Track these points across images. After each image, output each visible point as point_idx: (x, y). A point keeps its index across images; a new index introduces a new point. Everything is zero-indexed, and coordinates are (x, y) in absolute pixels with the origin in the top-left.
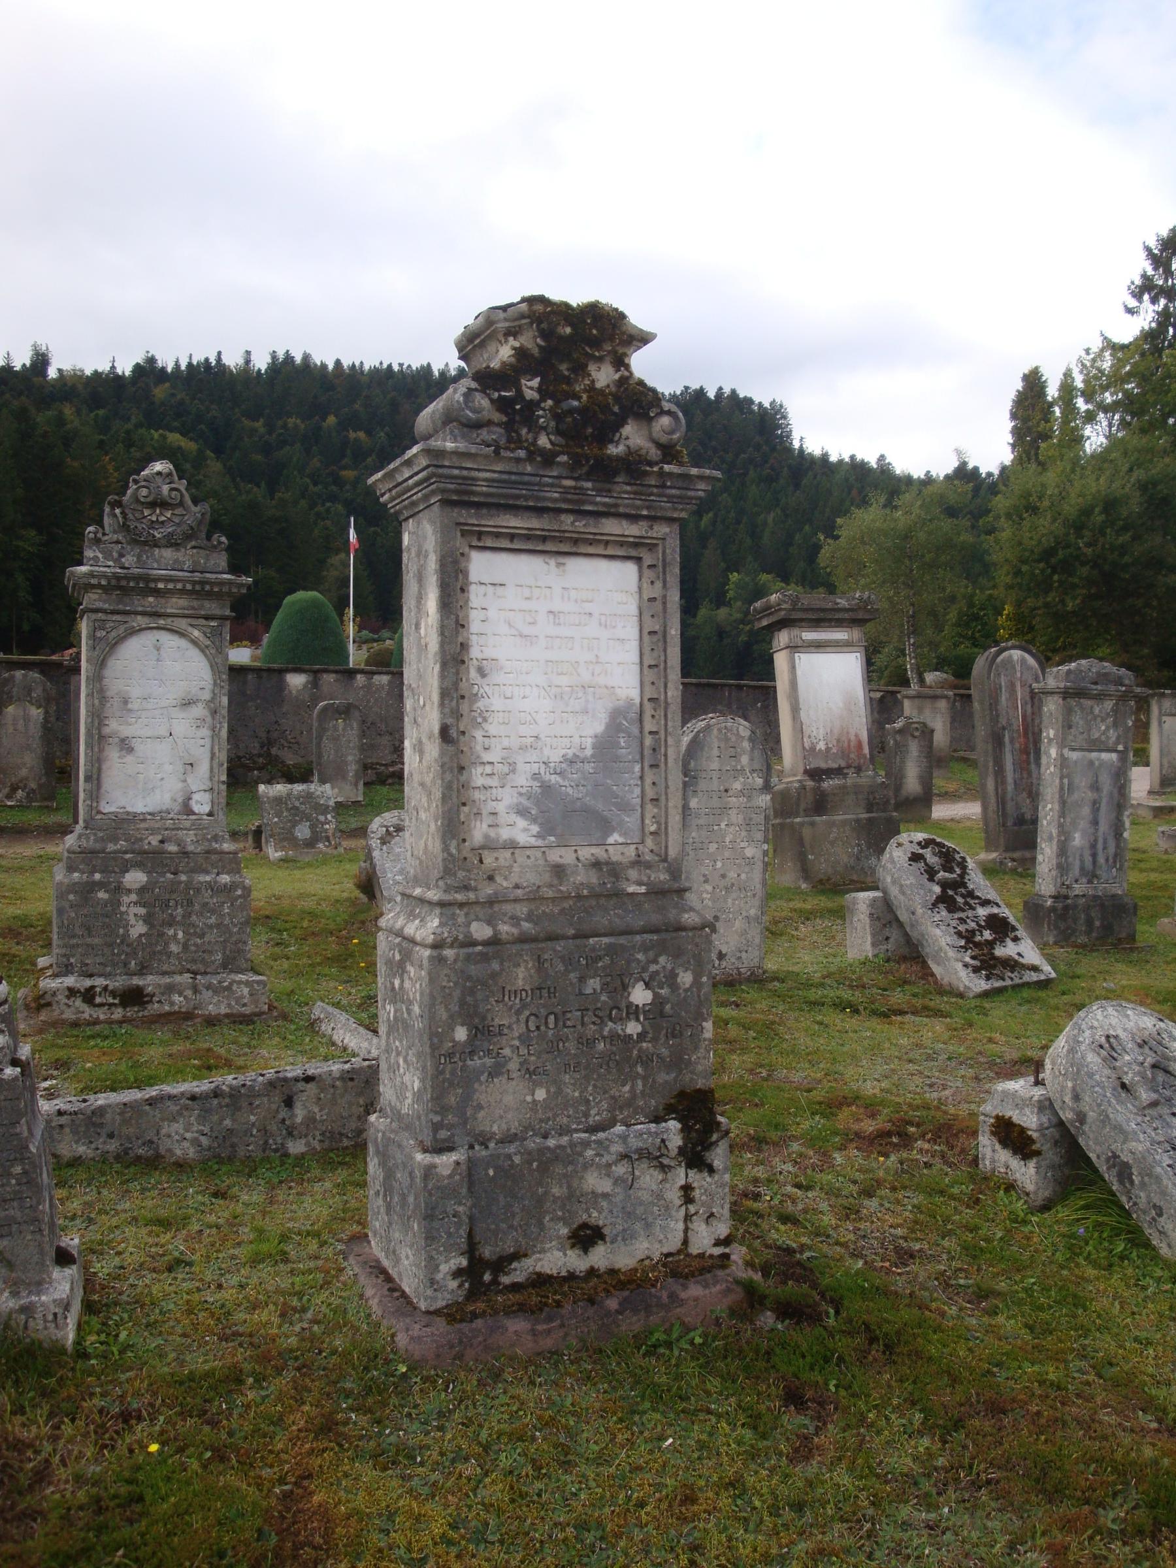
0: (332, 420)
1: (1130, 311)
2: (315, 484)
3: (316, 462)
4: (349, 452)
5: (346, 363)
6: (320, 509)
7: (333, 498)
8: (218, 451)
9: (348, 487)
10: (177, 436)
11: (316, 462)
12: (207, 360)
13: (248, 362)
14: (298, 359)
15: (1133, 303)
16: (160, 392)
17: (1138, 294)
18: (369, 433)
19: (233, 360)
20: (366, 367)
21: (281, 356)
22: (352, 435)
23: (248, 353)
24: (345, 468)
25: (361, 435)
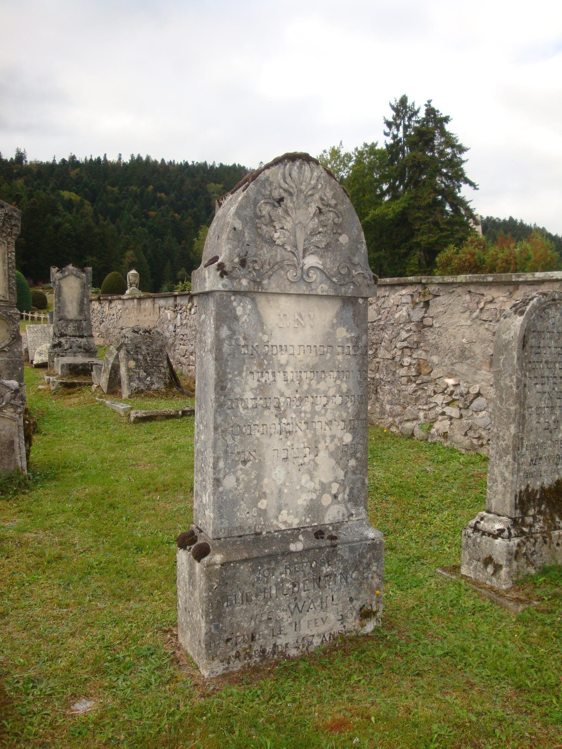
0: (151, 187)
1: (386, 134)
2: (135, 218)
3: (136, 207)
4: (156, 203)
5: (167, 161)
6: (134, 229)
7: (143, 225)
8: (93, 201)
9: (151, 219)
10: (73, 194)
11: (136, 207)
12: (99, 158)
13: (120, 159)
14: (144, 158)
15: (387, 130)
16: (73, 173)
17: (389, 124)
18: (167, 194)
19: (112, 158)
20: (176, 163)
21: (136, 157)
22: (159, 195)
23: (120, 155)
24: (153, 210)
25: (163, 195)
